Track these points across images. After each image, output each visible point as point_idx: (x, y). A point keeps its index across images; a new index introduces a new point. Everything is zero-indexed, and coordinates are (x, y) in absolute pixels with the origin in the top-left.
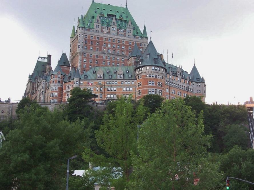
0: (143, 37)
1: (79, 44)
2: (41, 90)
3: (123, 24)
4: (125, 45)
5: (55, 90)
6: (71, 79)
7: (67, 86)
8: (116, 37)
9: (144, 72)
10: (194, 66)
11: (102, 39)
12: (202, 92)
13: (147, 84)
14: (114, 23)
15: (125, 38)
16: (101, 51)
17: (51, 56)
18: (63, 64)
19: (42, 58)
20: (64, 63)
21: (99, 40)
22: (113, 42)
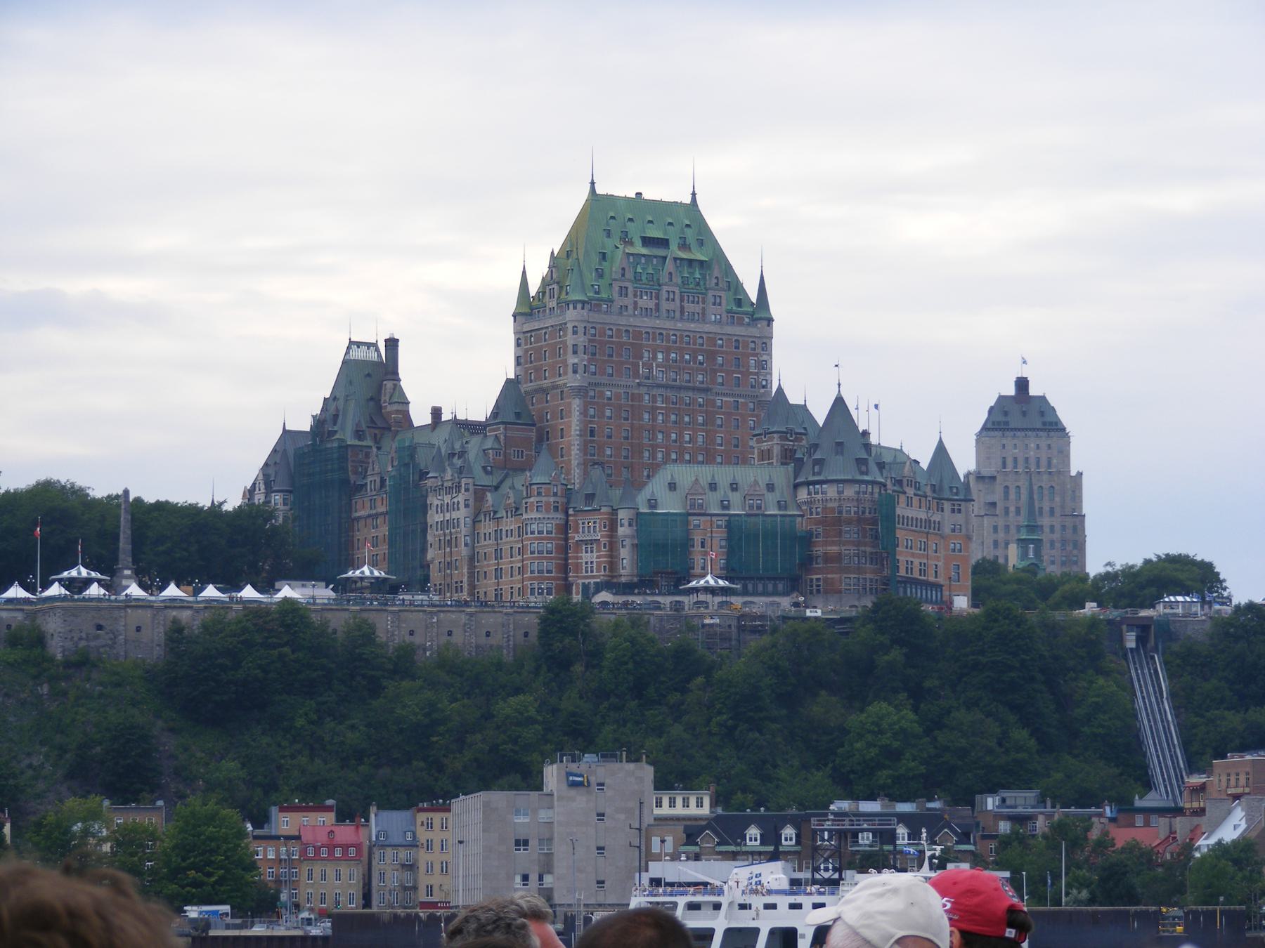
0: (761, 319)
1: (576, 361)
2: (454, 507)
3: (698, 276)
4: (706, 351)
5: (545, 532)
6: (596, 501)
7: (583, 523)
8: (679, 325)
9: (831, 499)
10: (941, 442)
11: (638, 335)
12: (967, 530)
14: (670, 273)
15: (707, 328)
16: (639, 379)
17: (398, 340)
18: (512, 419)
19: (359, 344)
20: (518, 415)
21: (631, 341)
22: (671, 344)
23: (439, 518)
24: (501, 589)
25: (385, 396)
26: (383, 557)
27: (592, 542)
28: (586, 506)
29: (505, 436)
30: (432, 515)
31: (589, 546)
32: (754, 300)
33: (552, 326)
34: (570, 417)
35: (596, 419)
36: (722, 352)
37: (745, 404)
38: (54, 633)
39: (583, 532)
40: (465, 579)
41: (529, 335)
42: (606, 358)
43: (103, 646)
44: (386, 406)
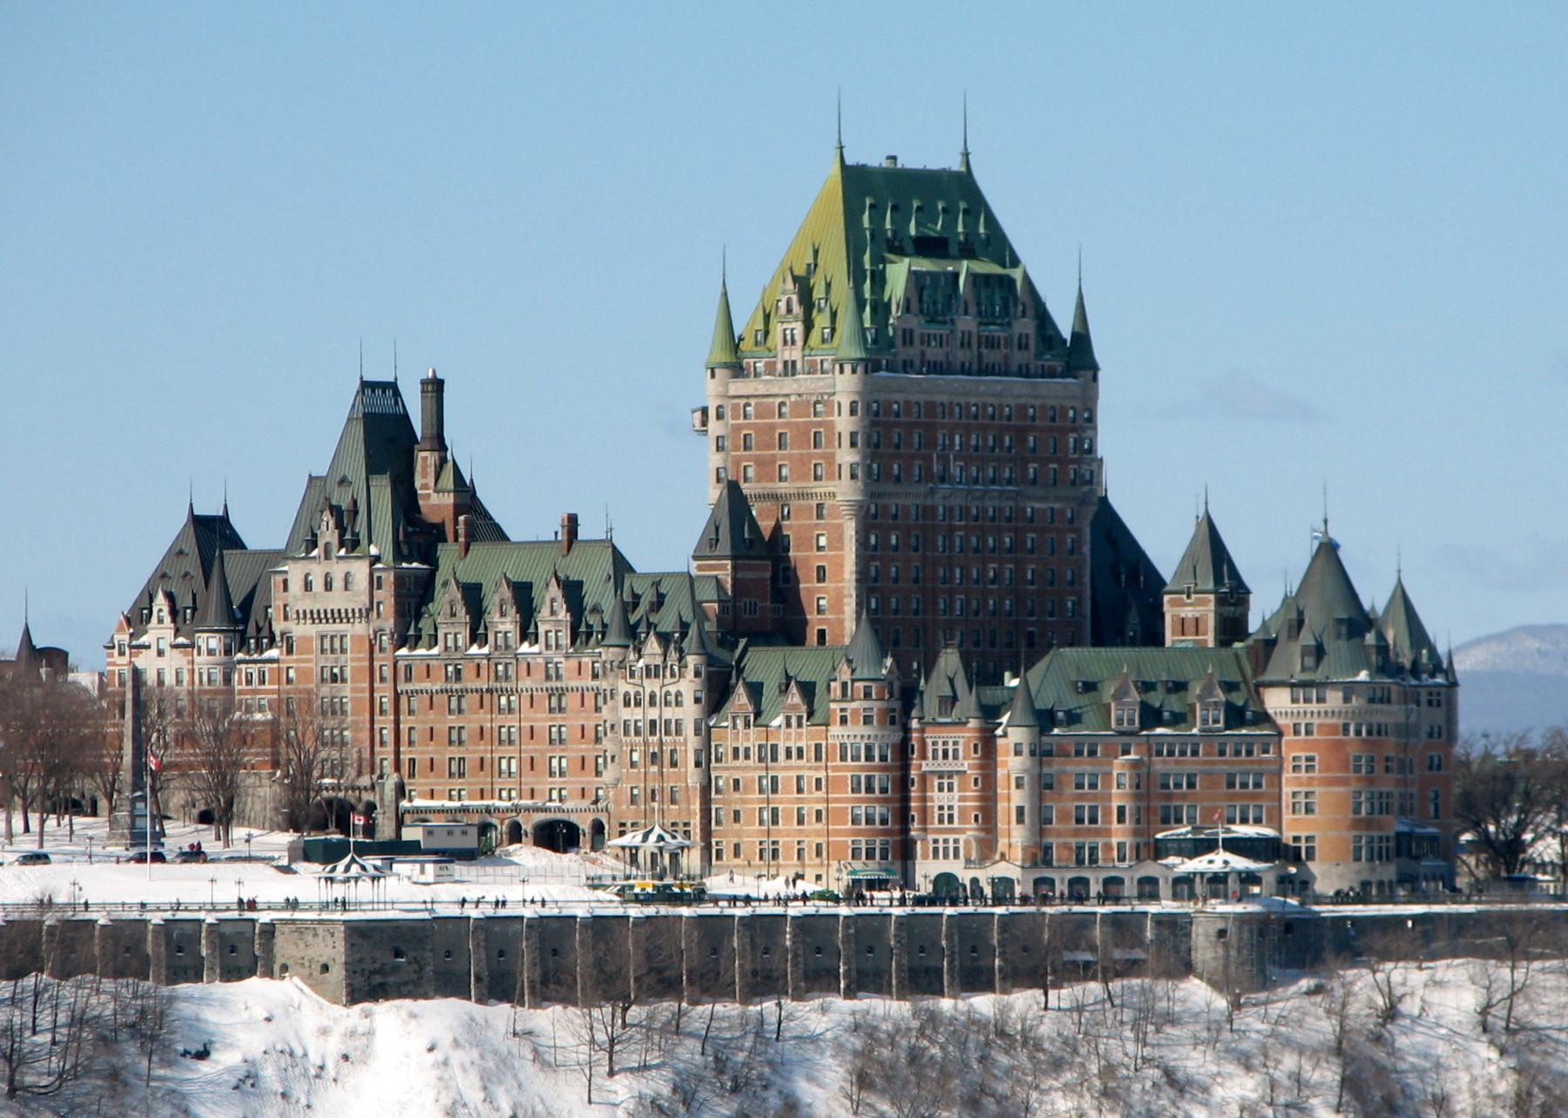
7: (934, 743)
10: (1400, 584)
11: (931, 407)
13: (1347, 770)
23: (632, 714)
24: (774, 843)
25: (425, 475)
26: (478, 764)
27: (950, 775)
28: (940, 714)
29: (734, 580)
30: (615, 709)
31: (946, 781)
32: (1066, 333)
33: (800, 395)
34: (842, 549)
35: (879, 553)
36: (1033, 428)
37: (1062, 511)
38: (330, 964)
39: (935, 757)
40: (696, 822)
41: (742, 402)
42: (892, 450)
43: (406, 983)
44: (429, 495)
